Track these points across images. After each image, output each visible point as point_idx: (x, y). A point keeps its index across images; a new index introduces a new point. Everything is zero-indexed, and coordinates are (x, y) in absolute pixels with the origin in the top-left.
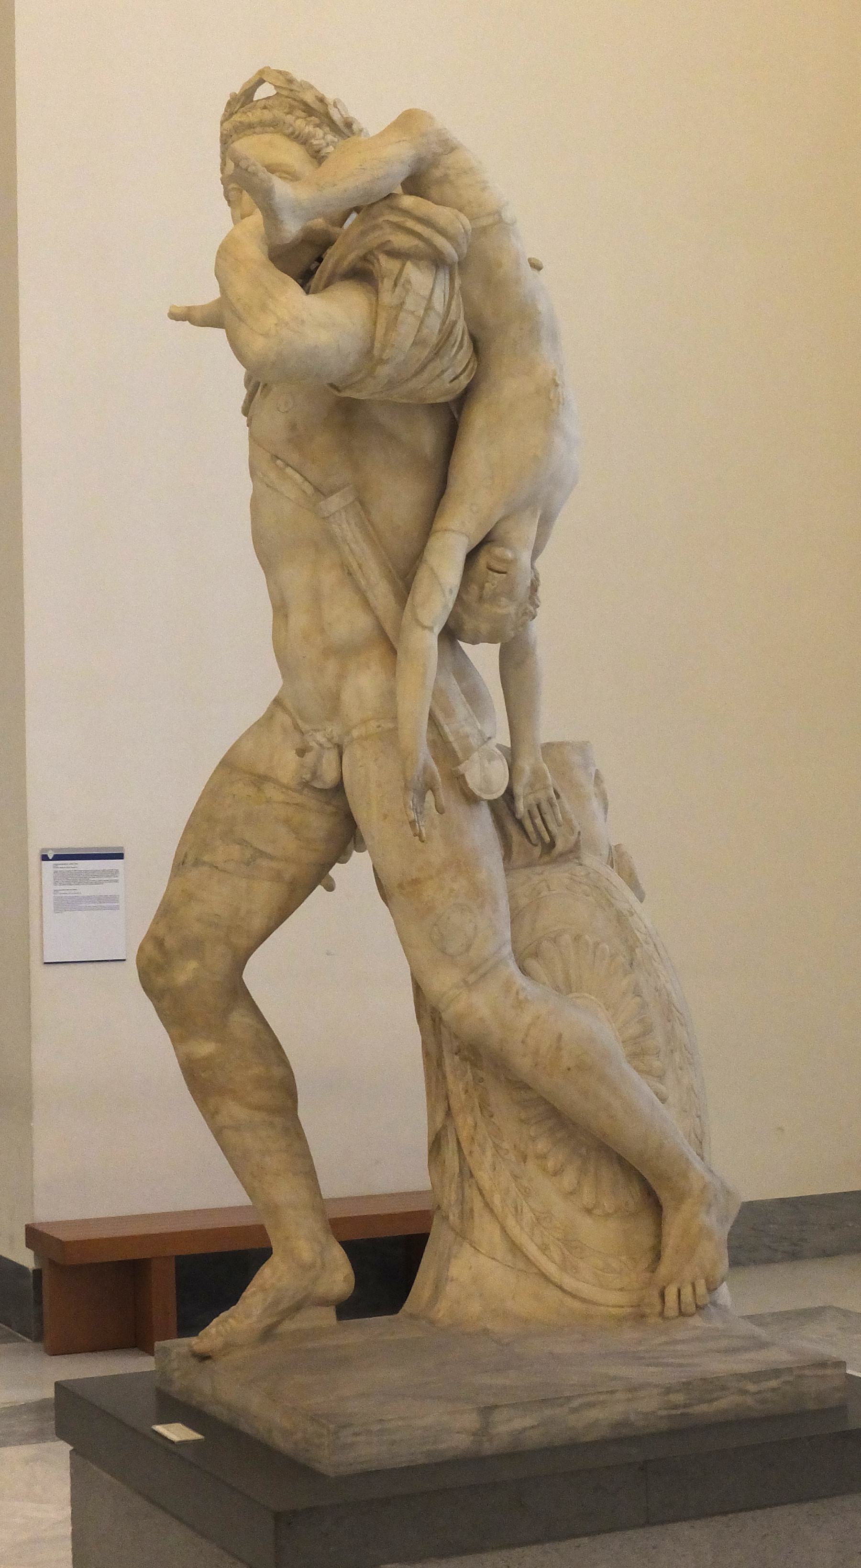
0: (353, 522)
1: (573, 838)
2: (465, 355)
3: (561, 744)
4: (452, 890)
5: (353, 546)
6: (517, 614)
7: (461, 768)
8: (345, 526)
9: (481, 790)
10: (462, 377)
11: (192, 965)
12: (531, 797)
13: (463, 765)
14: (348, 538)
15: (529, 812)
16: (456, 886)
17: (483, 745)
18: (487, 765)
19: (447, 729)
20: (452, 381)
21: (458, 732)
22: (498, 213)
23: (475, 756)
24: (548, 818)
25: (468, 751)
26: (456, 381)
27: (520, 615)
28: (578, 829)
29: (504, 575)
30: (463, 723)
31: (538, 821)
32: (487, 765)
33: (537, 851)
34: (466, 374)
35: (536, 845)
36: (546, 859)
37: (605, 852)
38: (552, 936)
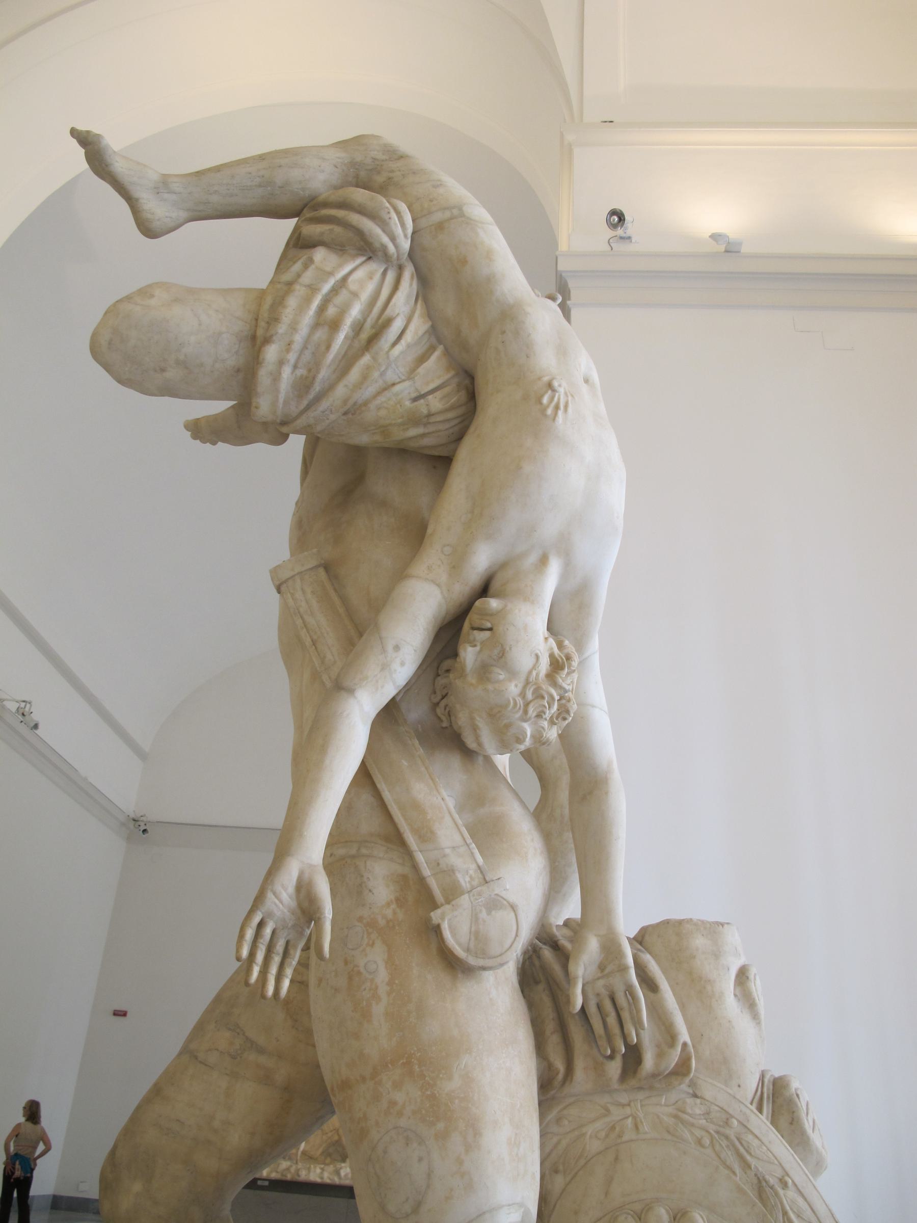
0: (308, 590)
1: (675, 1056)
2: (434, 371)
3: (680, 922)
4: (393, 1103)
5: (309, 619)
6: (523, 694)
7: (435, 916)
8: (299, 595)
9: (468, 950)
10: (430, 397)
11: (137, 1187)
12: (601, 983)
13: (439, 911)
14: (301, 610)
15: (599, 1007)
16: (399, 1097)
17: (480, 885)
18: (483, 914)
19: (420, 858)
20: (415, 400)
21: (438, 864)
22: (460, 208)
23: (464, 901)
24: (626, 1015)
25: (453, 892)
26: (422, 401)
27: (529, 696)
28: (684, 1036)
29: (488, 633)
30: (448, 851)
31: (612, 1020)
32: (483, 914)
33: (614, 1068)
34: (438, 394)
35: (611, 1057)
36: (633, 1082)
37: (751, 1084)
38: (638, 1207)
